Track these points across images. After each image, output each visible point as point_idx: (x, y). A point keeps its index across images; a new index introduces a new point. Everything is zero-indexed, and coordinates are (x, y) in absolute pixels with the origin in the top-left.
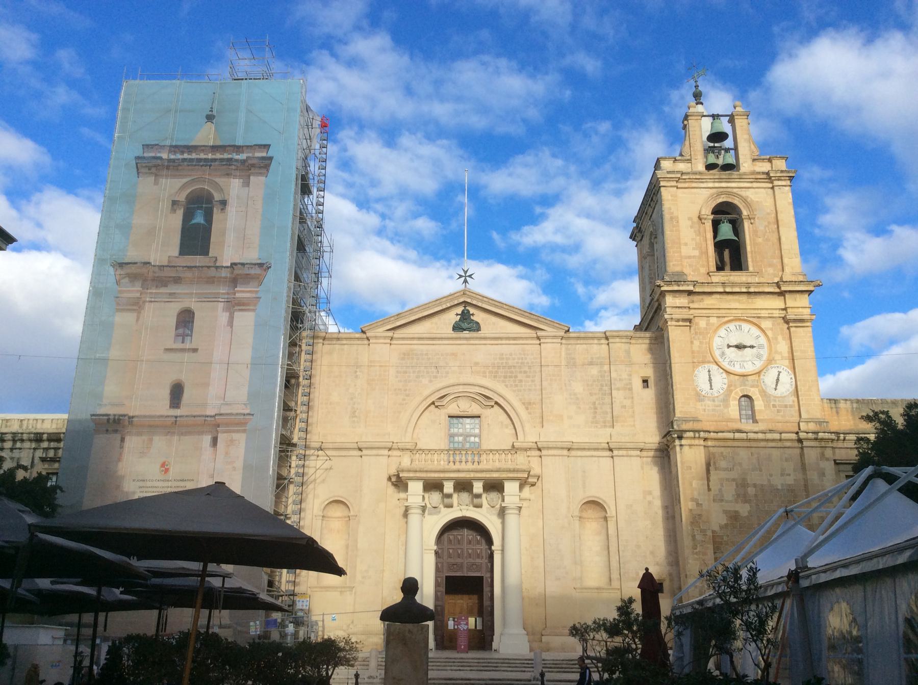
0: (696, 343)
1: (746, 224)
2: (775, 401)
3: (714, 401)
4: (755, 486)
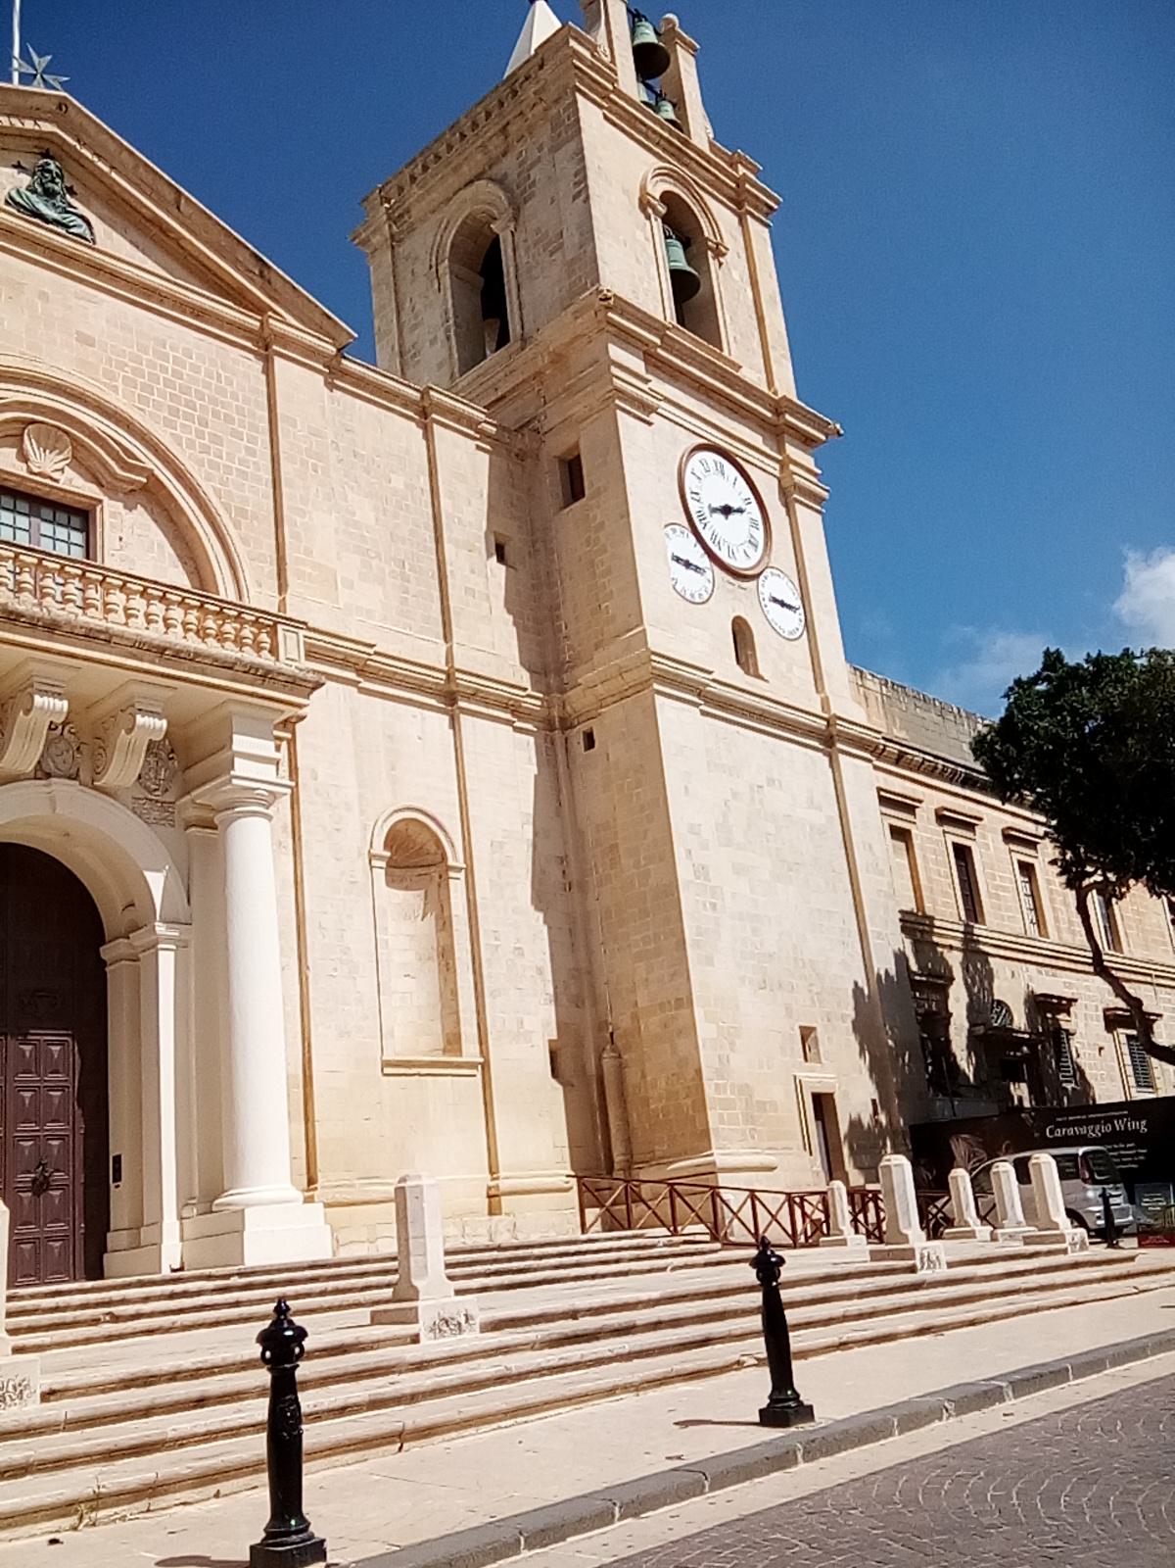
1: (713, 264)
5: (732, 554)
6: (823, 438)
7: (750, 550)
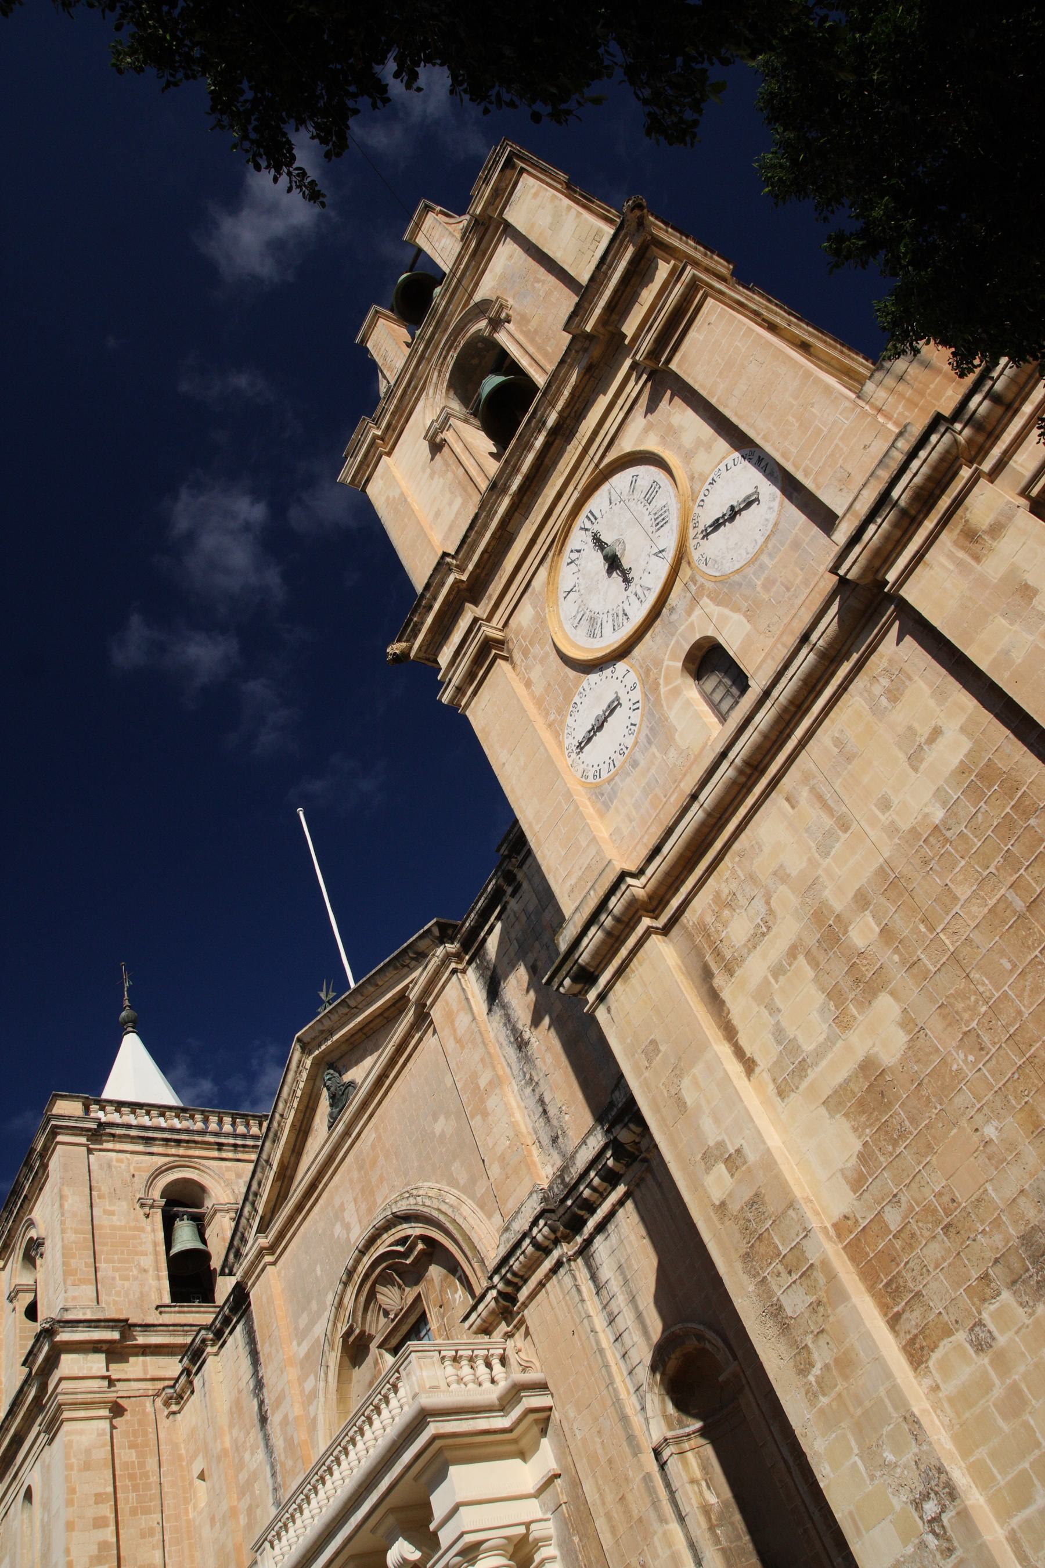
0: (535, 675)
2: (762, 567)
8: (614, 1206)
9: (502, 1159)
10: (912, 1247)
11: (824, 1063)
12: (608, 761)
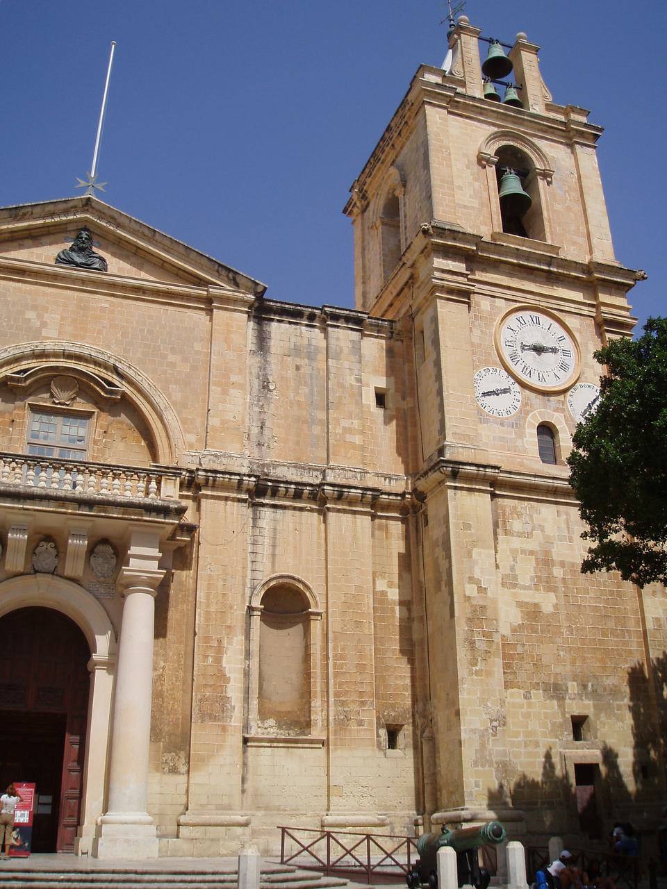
0: (477, 332)
1: (541, 183)
3: (502, 424)
4: (562, 564)
5: (541, 378)
6: (632, 283)
7: (561, 373)
8: (291, 506)
9: (223, 422)
10: (520, 660)
11: (522, 591)
12: (490, 408)
